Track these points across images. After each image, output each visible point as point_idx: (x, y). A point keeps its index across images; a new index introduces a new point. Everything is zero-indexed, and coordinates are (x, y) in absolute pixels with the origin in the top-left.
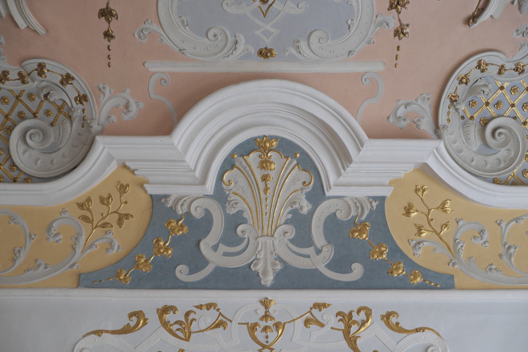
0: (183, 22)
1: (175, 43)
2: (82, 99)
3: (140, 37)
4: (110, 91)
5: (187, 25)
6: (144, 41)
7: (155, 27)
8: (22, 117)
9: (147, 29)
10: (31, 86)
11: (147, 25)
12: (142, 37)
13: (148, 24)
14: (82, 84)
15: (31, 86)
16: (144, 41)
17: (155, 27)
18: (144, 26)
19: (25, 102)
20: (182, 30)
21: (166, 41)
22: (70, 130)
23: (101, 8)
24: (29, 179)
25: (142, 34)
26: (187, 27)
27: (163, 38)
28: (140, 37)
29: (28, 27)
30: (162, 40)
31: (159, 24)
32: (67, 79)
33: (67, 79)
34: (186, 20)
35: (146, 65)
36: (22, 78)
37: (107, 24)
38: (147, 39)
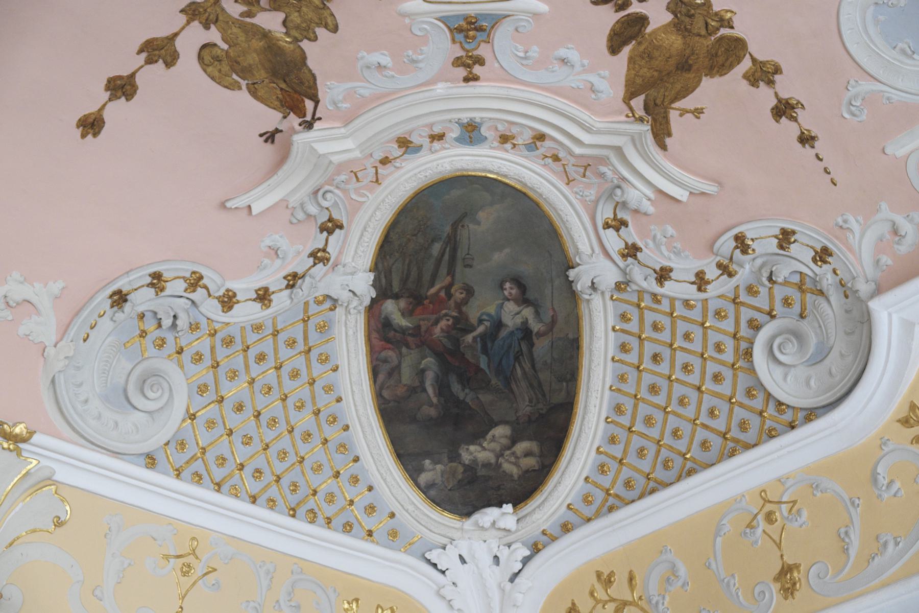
0: (903, 52)
1: (913, 91)
2: (822, 255)
3: (854, 115)
4: (857, 221)
5: (914, 53)
6: (864, 117)
7: (867, 86)
8: (755, 327)
9: (855, 97)
10: (745, 272)
11: (853, 91)
12: (857, 113)
13: (853, 87)
14: (811, 234)
15: (745, 272)
16: (864, 117)
17: (867, 86)
18: (849, 94)
19: (749, 302)
20: (911, 65)
21: (896, 96)
22: (832, 310)
23: (771, 107)
24: (811, 414)
25: (853, 109)
26: (915, 56)
27: (887, 95)
28: (854, 115)
29: (691, 193)
30: (888, 99)
31: (869, 78)
32: (785, 238)
33: (785, 238)
34: (906, 46)
35: (887, 151)
36: (725, 270)
37: (794, 124)
38: (866, 111)
